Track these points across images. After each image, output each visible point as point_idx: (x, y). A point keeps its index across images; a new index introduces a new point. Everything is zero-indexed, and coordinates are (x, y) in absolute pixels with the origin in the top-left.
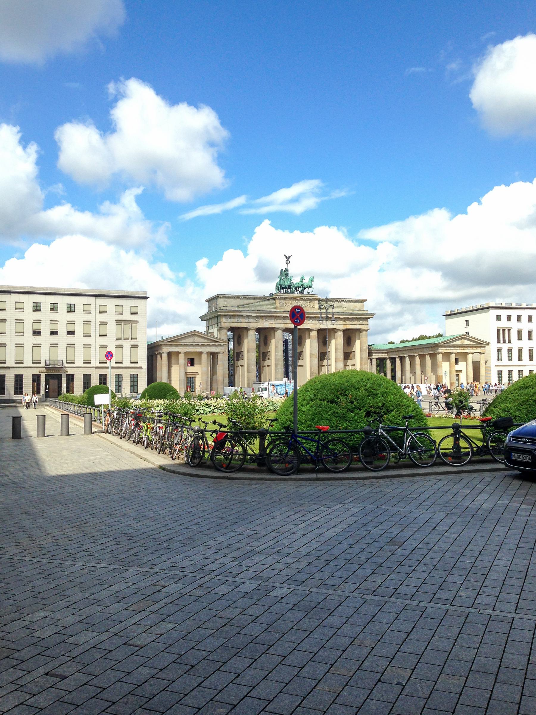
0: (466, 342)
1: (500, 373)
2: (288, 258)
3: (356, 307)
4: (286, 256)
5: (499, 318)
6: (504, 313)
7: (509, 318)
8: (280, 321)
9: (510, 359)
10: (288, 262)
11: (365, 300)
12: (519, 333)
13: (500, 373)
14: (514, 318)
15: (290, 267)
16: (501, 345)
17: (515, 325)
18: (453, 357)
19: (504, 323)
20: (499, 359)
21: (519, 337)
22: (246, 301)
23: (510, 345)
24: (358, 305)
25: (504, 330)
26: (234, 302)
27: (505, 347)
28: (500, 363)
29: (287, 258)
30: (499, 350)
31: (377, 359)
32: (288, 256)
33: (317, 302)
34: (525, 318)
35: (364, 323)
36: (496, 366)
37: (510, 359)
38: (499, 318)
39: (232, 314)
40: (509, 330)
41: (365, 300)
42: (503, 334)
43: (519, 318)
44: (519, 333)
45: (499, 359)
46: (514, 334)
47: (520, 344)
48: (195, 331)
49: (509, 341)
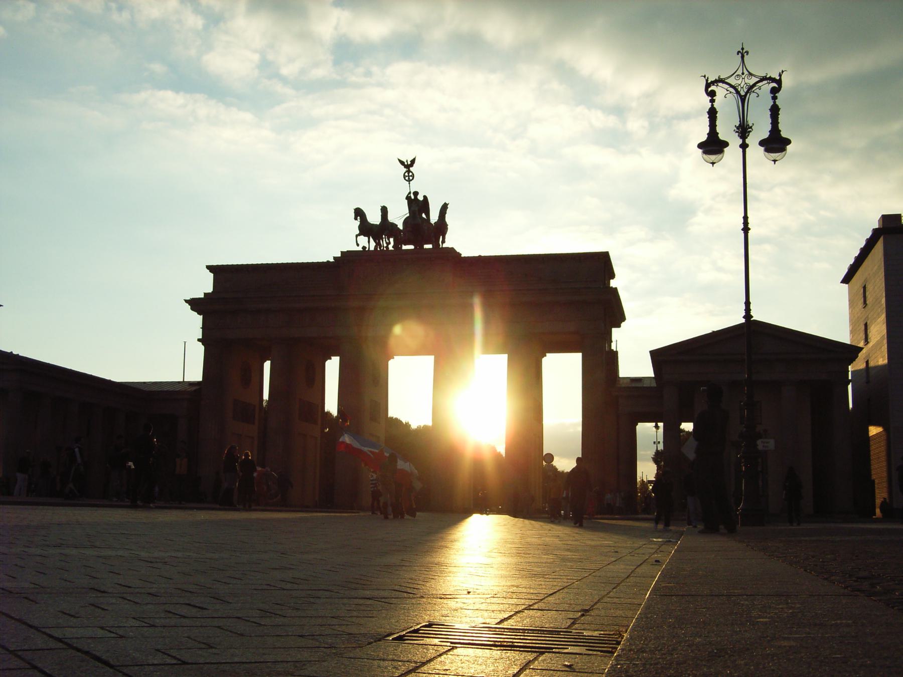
2: (408, 166)
4: (402, 163)
10: (409, 177)
32: (407, 159)
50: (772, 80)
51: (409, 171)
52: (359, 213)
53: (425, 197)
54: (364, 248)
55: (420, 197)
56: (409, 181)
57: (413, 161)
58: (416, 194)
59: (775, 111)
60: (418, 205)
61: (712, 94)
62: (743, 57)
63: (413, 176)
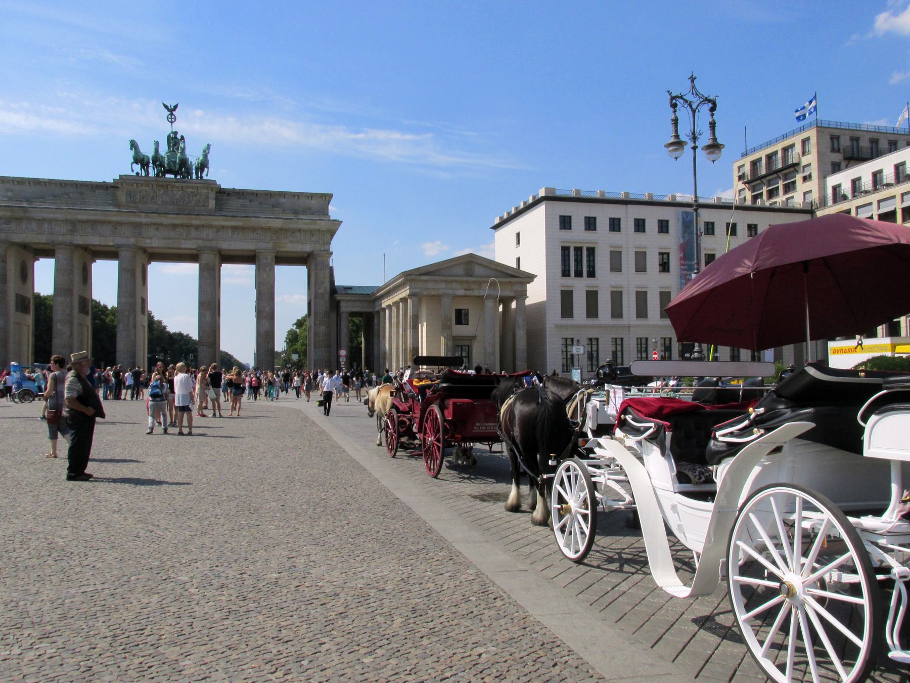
2: (172, 110)
4: (166, 107)
5: (566, 223)
6: (578, 213)
7: (590, 224)
10: (172, 119)
14: (603, 224)
15: (180, 127)
19: (578, 235)
21: (616, 265)
23: (591, 281)
27: (580, 287)
29: (169, 110)
31: (353, 314)
32: (171, 104)
33: (212, 195)
36: (556, 326)
40: (591, 251)
46: (602, 262)
47: (616, 280)
49: (592, 274)
50: (710, 101)
51: (172, 114)
52: (134, 145)
54: (138, 174)
55: (179, 137)
56: (172, 122)
57: (176, 107)
58: (176, 133)
59: (713, 125)
61: (674, 106)
62: (693, 81)
63: (175, 119)
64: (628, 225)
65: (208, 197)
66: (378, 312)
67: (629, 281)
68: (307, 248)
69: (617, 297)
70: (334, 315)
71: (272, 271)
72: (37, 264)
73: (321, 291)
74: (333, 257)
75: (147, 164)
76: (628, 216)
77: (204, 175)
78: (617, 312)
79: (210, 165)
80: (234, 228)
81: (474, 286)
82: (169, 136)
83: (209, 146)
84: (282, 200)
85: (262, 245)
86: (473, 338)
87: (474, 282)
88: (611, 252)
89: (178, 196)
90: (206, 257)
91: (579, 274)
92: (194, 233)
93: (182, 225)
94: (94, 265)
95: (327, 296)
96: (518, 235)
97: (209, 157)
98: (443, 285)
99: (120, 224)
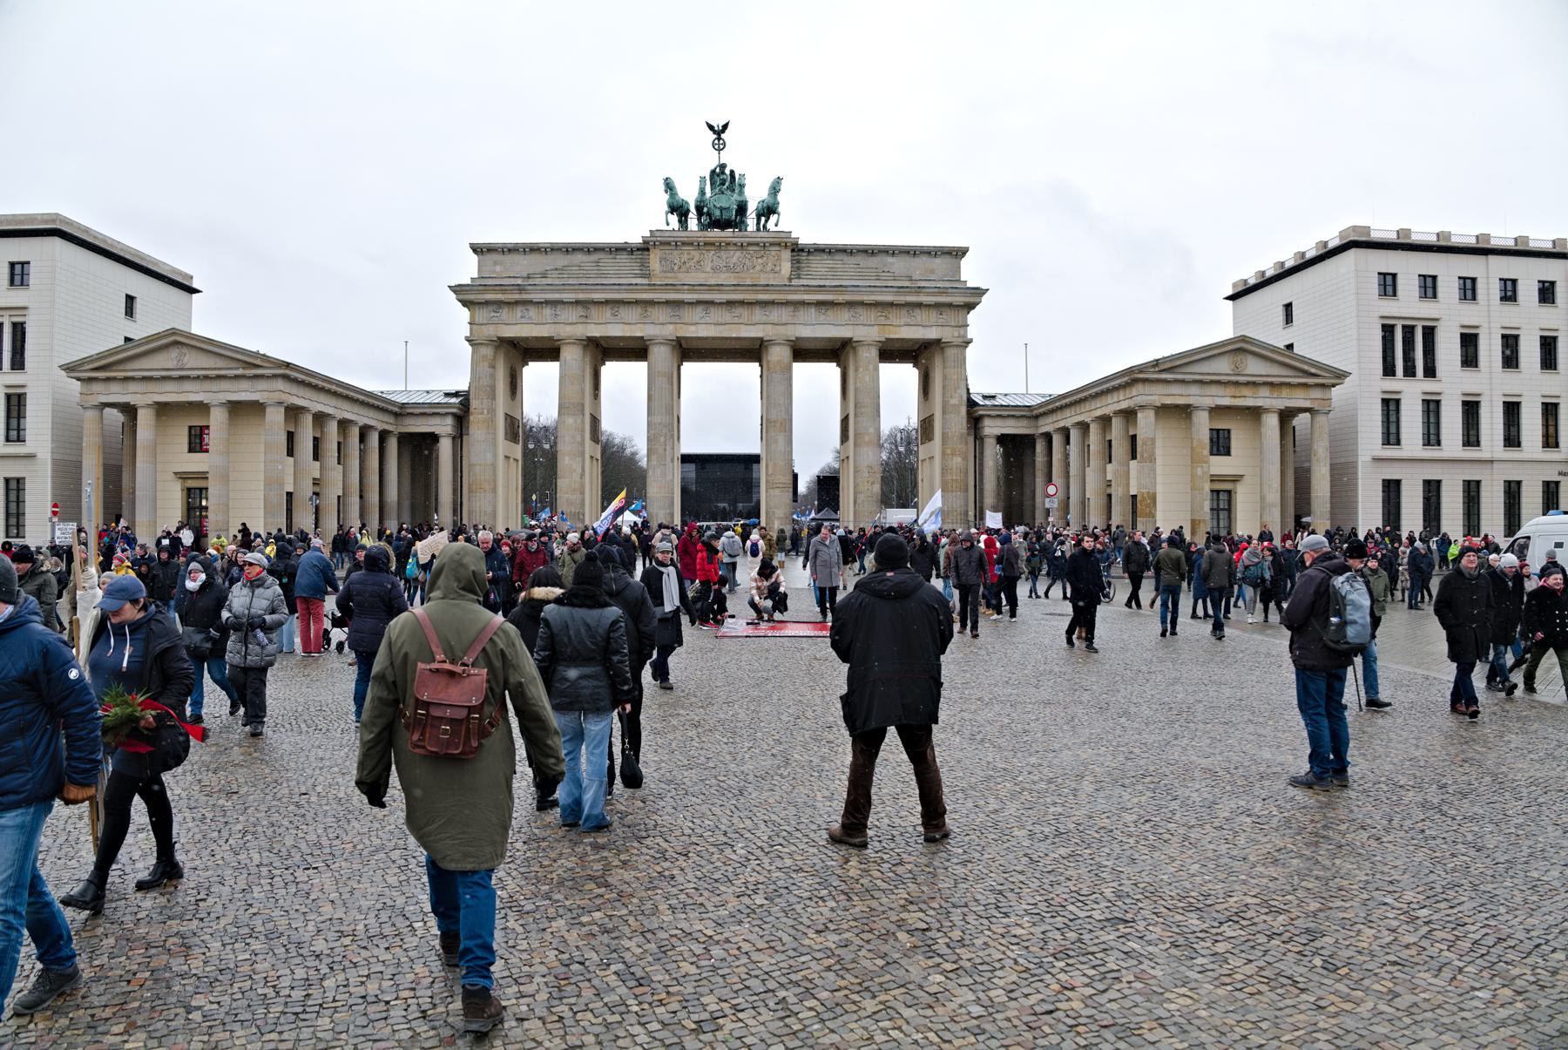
0: (1254, 368)
1: (1392, 489)
2: (719, 132)
3: (932, 272)
4: (711, 127)
5: (1388, 285)
6: (1408, 268)
7: (1429, 286)
8: (660, 314)
9: (1432, 436)
10: (719, 144)
11: (963, 252)
12: (1469, 342)
13: (1392, 489)
14: (1448, 288)
15: (734, 159)
16: (1399, 384)
17: (1450, 316)
18: (1203, 425)
19: (1408, 305)
20: (1391, 435)
21: (1470, 358)
22: (561, 260)
23: (1430, 386)
24: (939, 263)
25: (1409, 331)
26: (523, 265)
27: (1412, 392)
28: (1391, 452)
30: (1391, 406)
31: (1002, 439)
32: (718, 123)
33: (787, 254)
34: (1489, 290)
35: (950, 317)
36: (1376, 460)
37: (1432, 436)
38: (1388, 285)
39: (499, 297)
40: (1429, 333)
41: (963, 252)
42: (1406, 347)
43: (1469, 288)
44: (1469, 342)
45: (1391, 435)
46: (1448, 350)
47: (1471, 382)
48: (173, 332)
49: (1430, 372)
52: (669, 186)
53: (732, 172)
55: (727, 171)
56: (719, 150)
57: (725, 127)
60: (723, 179)
64: (1489, 290)
65: (779, 259)
66: (1048, 437)
67: (1491, 383)
68: (931, 334)
69: (1471, 409)
70: (971, 439)
71: (877, 369)
72: (525, 369)
73: (954, 401)
74: (970, 351)
75: (688, 211)
76: (1490, 273)
77: (771, 225)
78: (1471, 436)
79: (780, 209)
80: (820, 304)
81: (1246, 391)
82: (713, 172)
83: (779, 180)
84: (890, 259)
85: (866, 330)
86: (1236, 479)
87: (1248, 384)
88: (1462, 335)
89: (734, 260)
90: (778, 354)
91: (1410, 371)
92: (758, 314)
93: (742, 303)
94: (603, 369)
95: (964, 410)
96: (1288, 307)
97: (780, 197)
98: (1194, 389)
99: (652, 303)
